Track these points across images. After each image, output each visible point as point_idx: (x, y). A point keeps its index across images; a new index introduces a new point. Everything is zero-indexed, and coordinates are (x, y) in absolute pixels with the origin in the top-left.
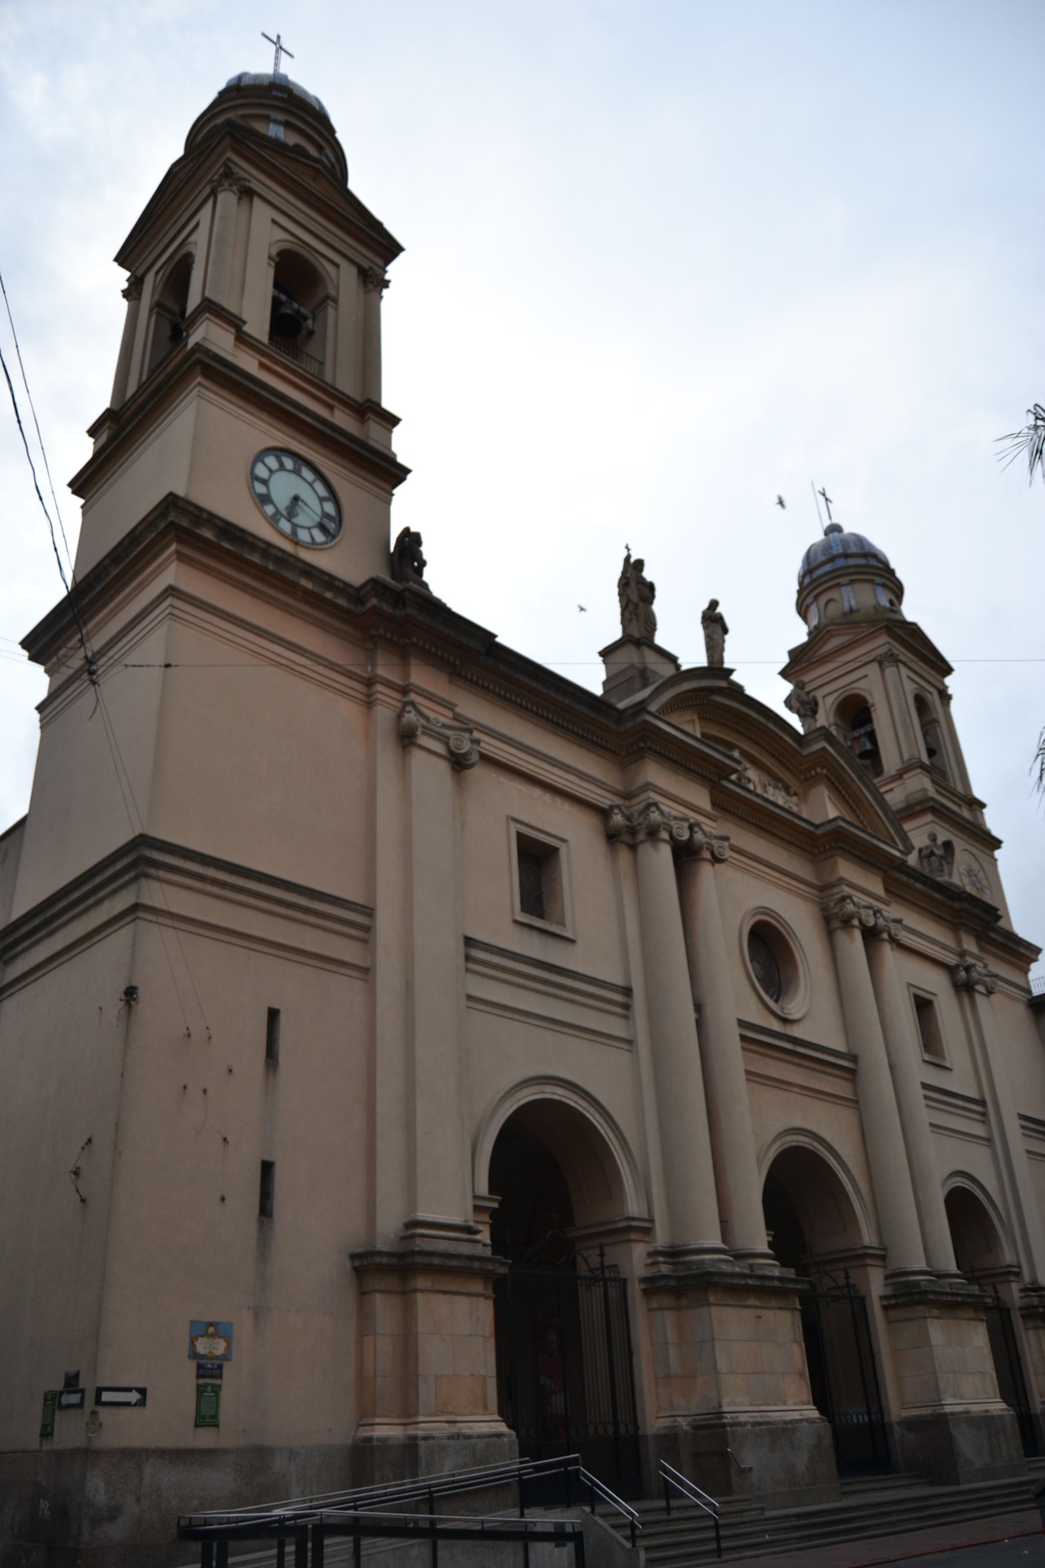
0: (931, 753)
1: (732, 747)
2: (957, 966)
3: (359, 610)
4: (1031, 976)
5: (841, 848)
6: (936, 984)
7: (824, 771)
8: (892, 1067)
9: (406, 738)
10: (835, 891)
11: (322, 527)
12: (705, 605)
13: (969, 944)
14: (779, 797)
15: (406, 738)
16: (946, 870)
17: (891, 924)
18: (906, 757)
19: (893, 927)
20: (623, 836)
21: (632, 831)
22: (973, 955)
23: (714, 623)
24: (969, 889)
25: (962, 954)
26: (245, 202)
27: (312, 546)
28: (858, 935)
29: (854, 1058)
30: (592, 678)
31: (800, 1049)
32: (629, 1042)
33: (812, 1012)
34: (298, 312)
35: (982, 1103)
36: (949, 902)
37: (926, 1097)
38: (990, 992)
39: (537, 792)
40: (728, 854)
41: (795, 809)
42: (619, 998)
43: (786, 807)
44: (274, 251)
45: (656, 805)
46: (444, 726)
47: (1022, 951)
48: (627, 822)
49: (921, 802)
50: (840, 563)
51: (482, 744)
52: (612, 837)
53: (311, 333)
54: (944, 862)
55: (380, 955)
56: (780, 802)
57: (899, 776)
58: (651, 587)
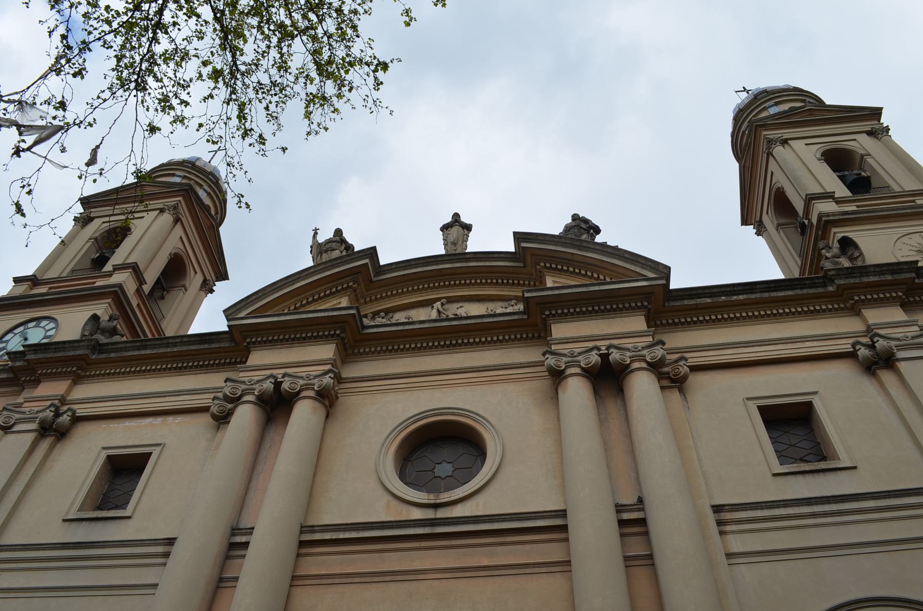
36: (820, 290)
42: (160, 549)
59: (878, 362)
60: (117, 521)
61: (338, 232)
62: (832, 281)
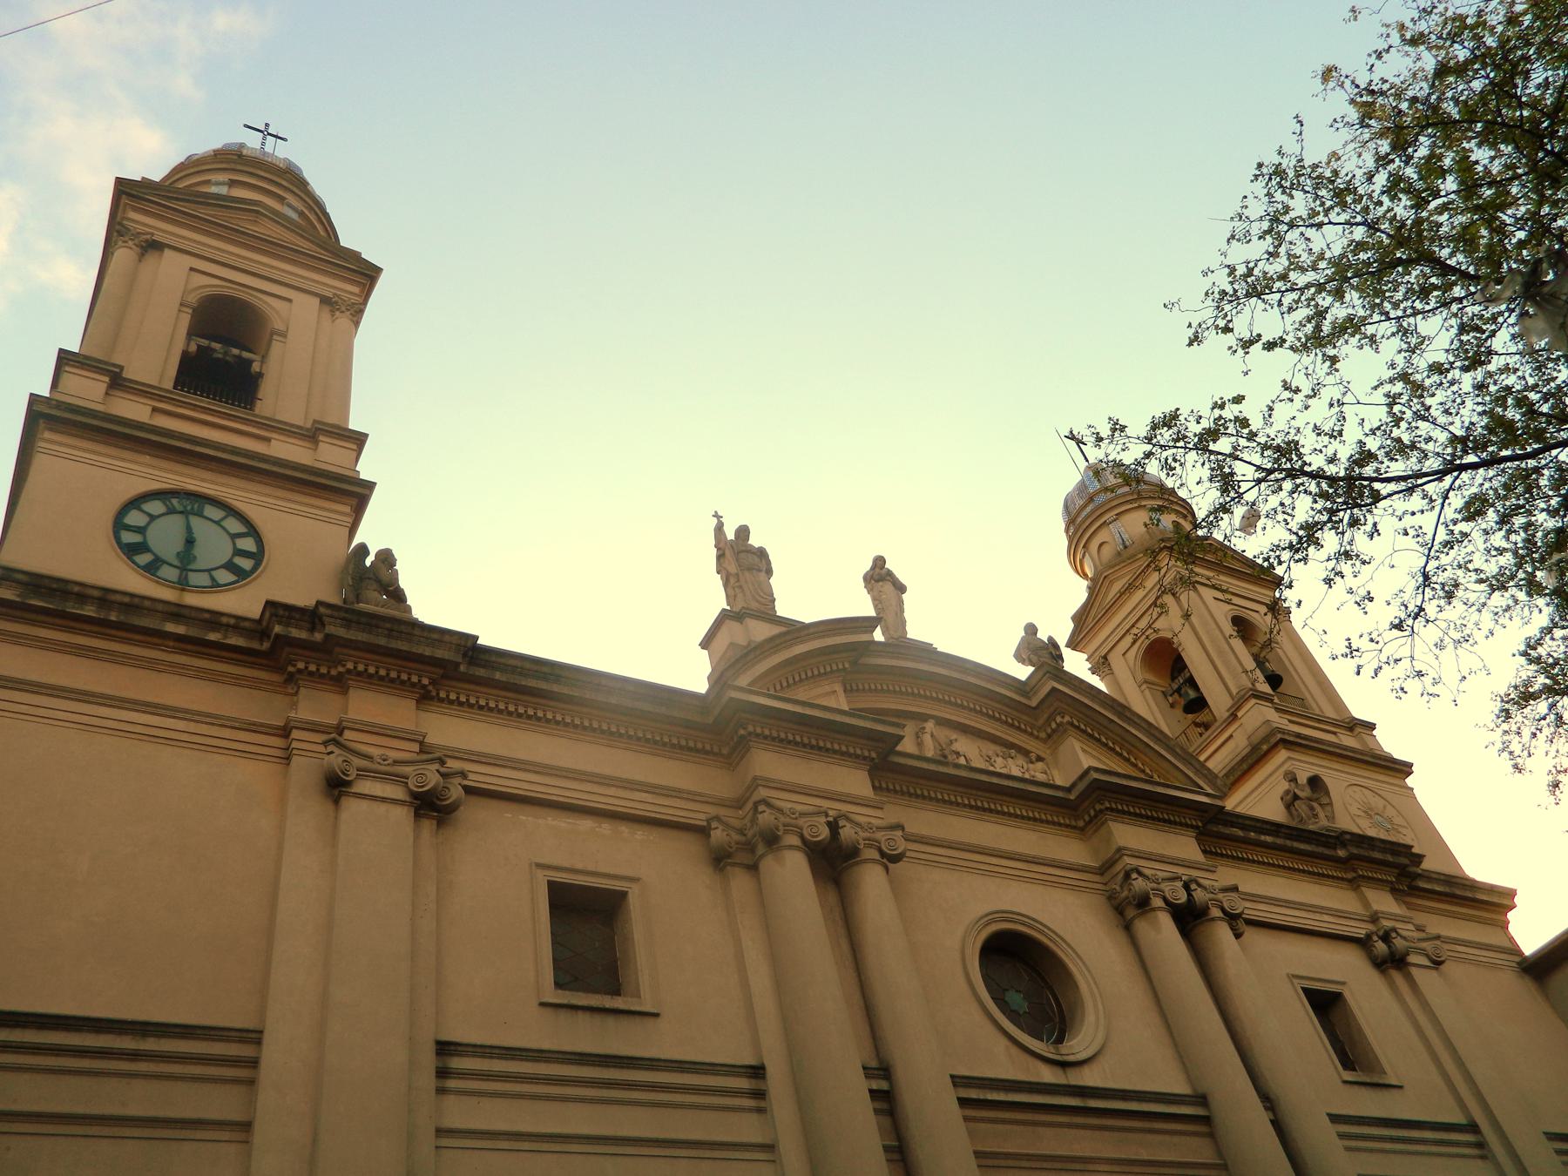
0: (1275, 680)
1: (924, 718)
2: (1369, 936)
3: (266, 646)
4: (1513, 929)
5: (1112, 810)
6: (1344, 969)
7: (1067, 718)
8: (1268, 1101)
9: (336, 786)
10: (1118, 867)
11: (230, 566)
12: (868, 565)
13: (1383, 902)
14: (1015, 767)
15: (336, 786)
16: (1322, 815)
17: (1220, 896)
18: (1234, 692)
19: (1227, 900)
20: (736, 852)
21: (749, 847)
22: (1395, 918)
23: (880, 578)
24: (1372, 833)
25: (1374, 918)
26: (151, 259)
27: (215, 586)
28: (1166, 921)
29: (1202, 1099)
30: (691, 673)
31: (1093, 1103)
32: (770, 1148)
33: (1120, 1040)
34: (239, 357)
35: (1473, 1128)
36: (1327, 852)
37: (1342, 1136)
38: (1437, 964)
39: (586, 824)
40: (902, 846)
41: (1041, 777)
42: (743, 1083)
43: (1027, 776)
44: (193, 299)
45: (765, 802)
46: (396, 762)
47: (1480, 896)
48: (736, 837)
49: (1265, 740)
50: (1102, 498)
51: (471, 776)
52: (720, 860)
53: (260, 375)
54: (1315, 805)
55: (267, 1097)
56: (1016, 772)
57: (1234, 717)
58: (762, 553)
59: (1392, 962)
60: (638, 1019)
61: (743, 532)
62: (1344, 845)
